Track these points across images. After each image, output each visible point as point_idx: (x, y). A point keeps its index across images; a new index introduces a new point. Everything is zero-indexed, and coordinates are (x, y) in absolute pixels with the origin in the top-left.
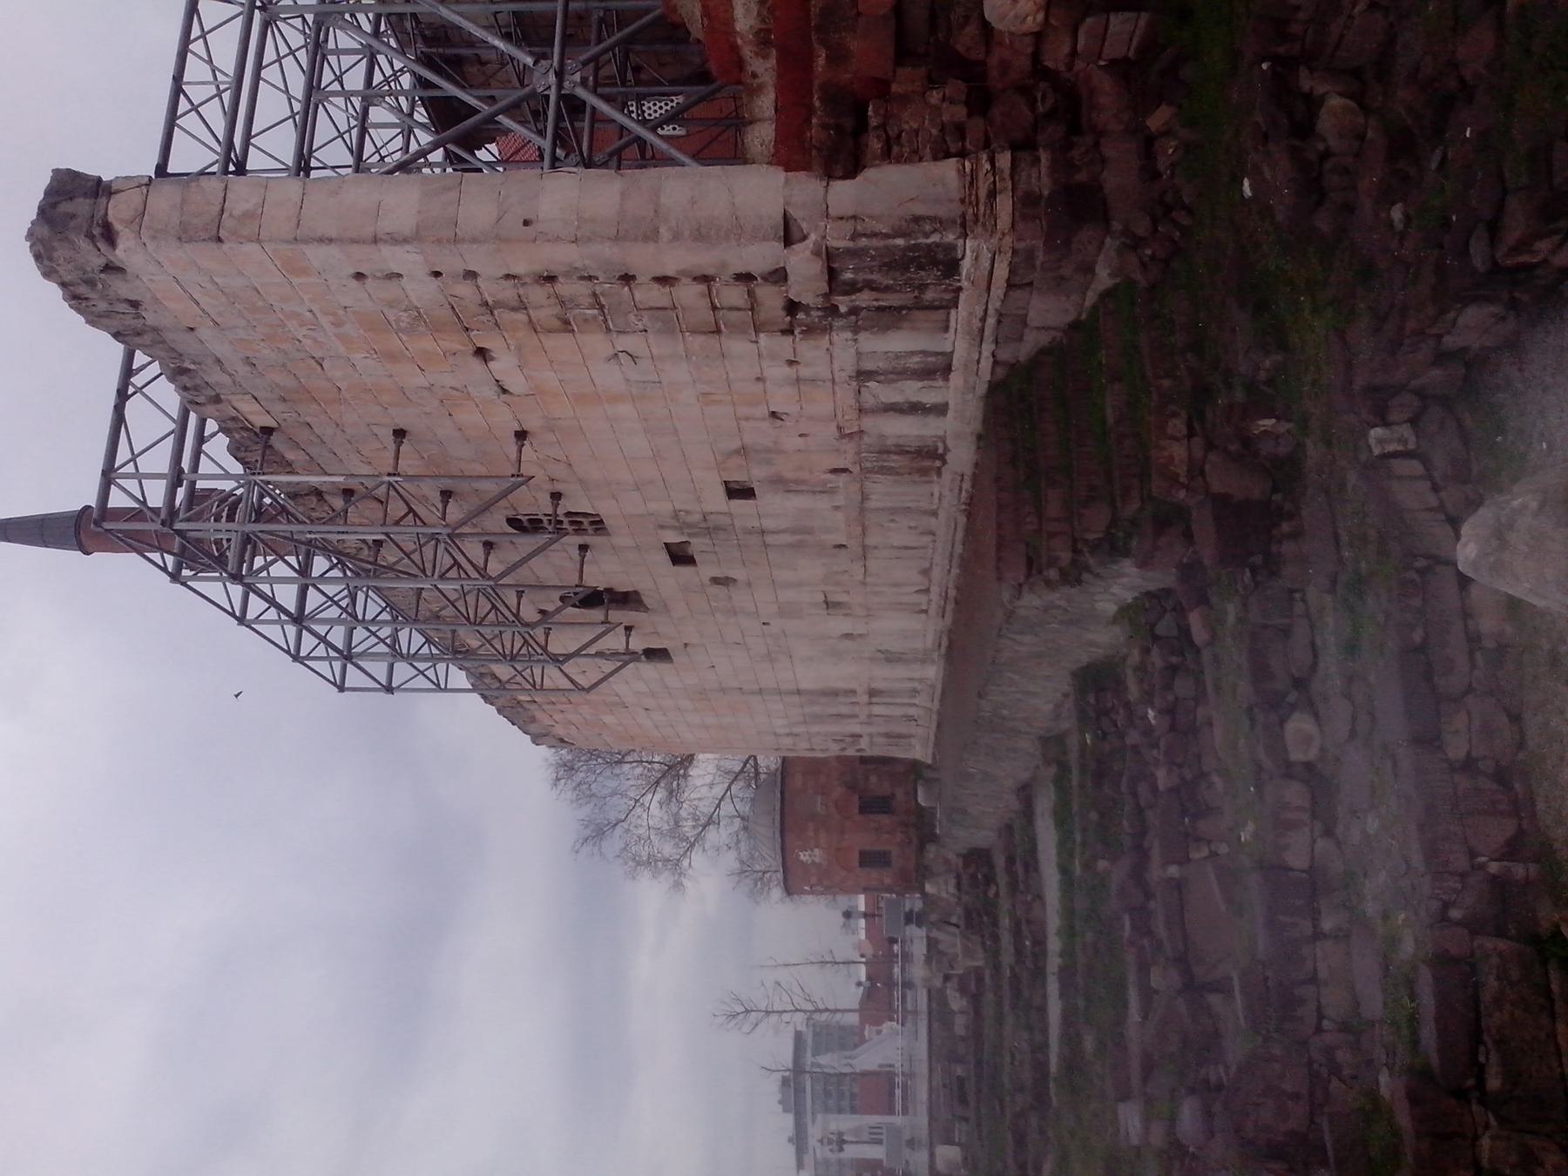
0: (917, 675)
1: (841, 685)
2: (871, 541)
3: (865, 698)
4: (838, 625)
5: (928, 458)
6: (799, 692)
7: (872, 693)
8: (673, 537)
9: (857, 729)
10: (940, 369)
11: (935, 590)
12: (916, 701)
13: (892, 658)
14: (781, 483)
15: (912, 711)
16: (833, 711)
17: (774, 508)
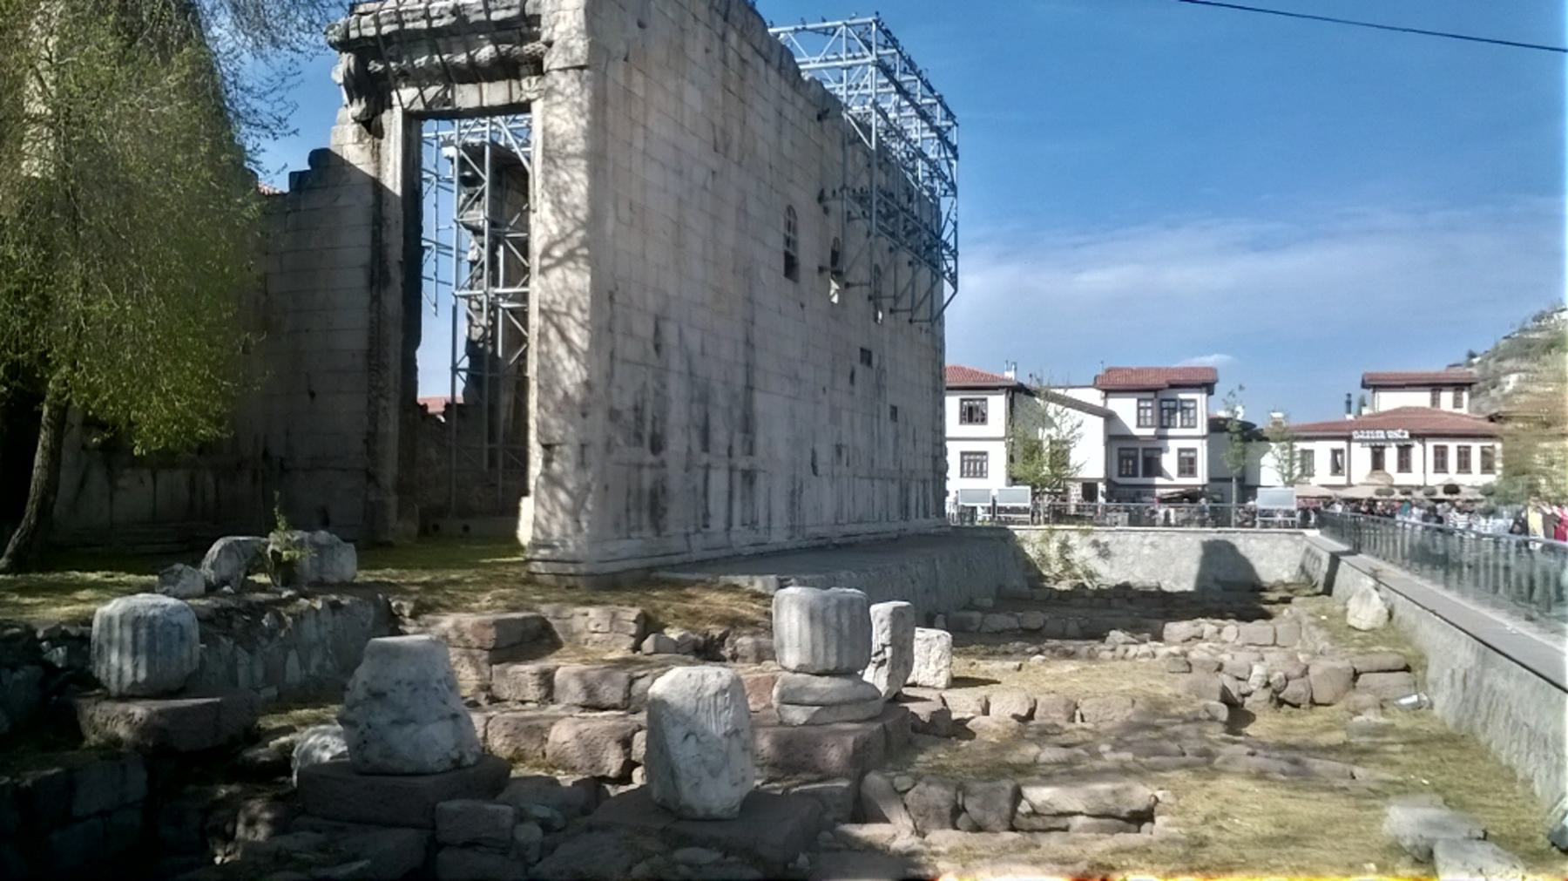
0: (776, 524)
1: (761, 440)
2: (877, 482)
3: (742, 463)
4: (825, 455)
5: (905, 509)
6: (749, 388)
7: (749, 476)
8: (875, 361)
9: (677, 444)
10: (926, 516)
11: (849, 529)
13: (794, 497)
14: (897, 438)
15: (717, 524)
16: (717, 421)
17: (888, 429)
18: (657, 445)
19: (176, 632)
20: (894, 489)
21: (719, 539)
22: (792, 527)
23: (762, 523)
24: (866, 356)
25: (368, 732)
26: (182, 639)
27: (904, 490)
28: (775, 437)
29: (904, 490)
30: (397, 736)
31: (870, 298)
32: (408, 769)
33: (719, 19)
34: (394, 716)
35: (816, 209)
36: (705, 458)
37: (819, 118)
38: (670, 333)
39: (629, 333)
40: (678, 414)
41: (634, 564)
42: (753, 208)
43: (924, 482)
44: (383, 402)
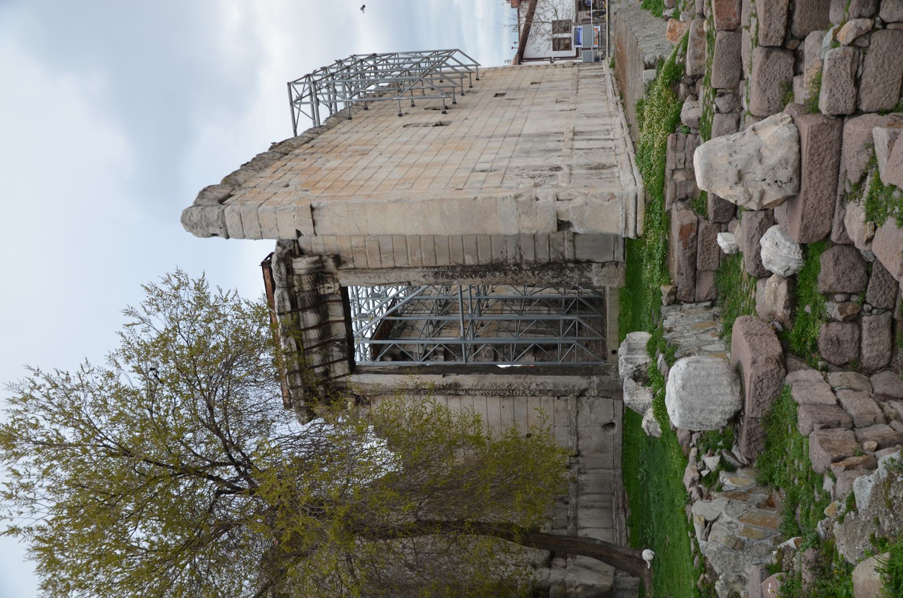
9: (555, 161)
11: (610, 95)
12: (611, 136)
15: (610, 144)
16: (542, 146)
18: (558, 168)
19: (694, 365)
20: (583, 81)
21: (620, 143)
22: (610, 116)
23: (609, 127)
24: (496, 95)
25: (768, 181)
26: (698, 362)
27: (585, 77)
28: (549, 125)
29: (585, 77)
30: (772, 159)
31: (463, 95)
32: (796, 149)
33: (286, 157)
34: (755, 162)
35: (404, 118)
36: (566, 151)
37: (350, 118)
38: (481, 166)
39: (484, 182)
40: (537, 161)
41: (636, 171)
42: (404, 139)
43: (579, 70)
44: (533, 386)
